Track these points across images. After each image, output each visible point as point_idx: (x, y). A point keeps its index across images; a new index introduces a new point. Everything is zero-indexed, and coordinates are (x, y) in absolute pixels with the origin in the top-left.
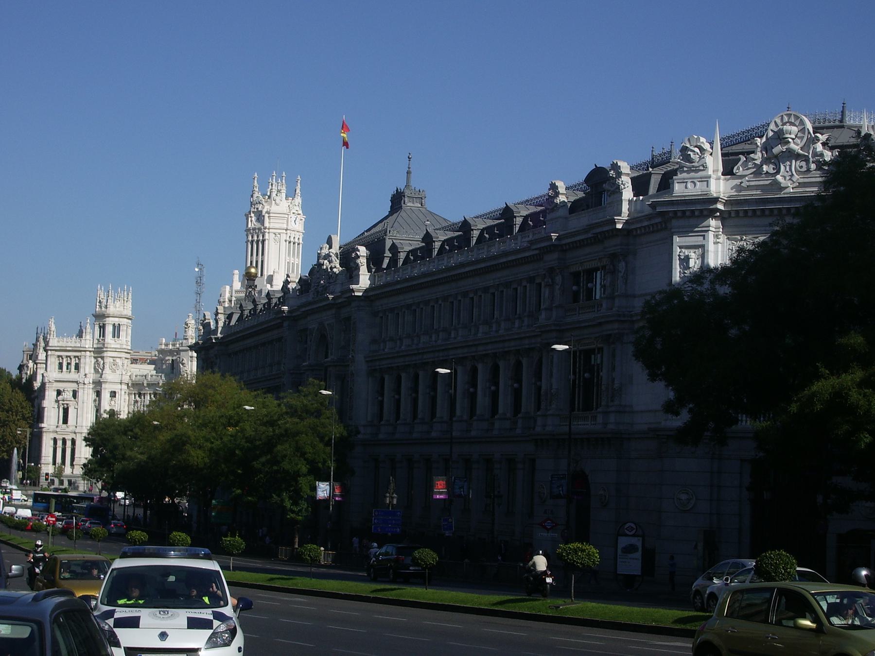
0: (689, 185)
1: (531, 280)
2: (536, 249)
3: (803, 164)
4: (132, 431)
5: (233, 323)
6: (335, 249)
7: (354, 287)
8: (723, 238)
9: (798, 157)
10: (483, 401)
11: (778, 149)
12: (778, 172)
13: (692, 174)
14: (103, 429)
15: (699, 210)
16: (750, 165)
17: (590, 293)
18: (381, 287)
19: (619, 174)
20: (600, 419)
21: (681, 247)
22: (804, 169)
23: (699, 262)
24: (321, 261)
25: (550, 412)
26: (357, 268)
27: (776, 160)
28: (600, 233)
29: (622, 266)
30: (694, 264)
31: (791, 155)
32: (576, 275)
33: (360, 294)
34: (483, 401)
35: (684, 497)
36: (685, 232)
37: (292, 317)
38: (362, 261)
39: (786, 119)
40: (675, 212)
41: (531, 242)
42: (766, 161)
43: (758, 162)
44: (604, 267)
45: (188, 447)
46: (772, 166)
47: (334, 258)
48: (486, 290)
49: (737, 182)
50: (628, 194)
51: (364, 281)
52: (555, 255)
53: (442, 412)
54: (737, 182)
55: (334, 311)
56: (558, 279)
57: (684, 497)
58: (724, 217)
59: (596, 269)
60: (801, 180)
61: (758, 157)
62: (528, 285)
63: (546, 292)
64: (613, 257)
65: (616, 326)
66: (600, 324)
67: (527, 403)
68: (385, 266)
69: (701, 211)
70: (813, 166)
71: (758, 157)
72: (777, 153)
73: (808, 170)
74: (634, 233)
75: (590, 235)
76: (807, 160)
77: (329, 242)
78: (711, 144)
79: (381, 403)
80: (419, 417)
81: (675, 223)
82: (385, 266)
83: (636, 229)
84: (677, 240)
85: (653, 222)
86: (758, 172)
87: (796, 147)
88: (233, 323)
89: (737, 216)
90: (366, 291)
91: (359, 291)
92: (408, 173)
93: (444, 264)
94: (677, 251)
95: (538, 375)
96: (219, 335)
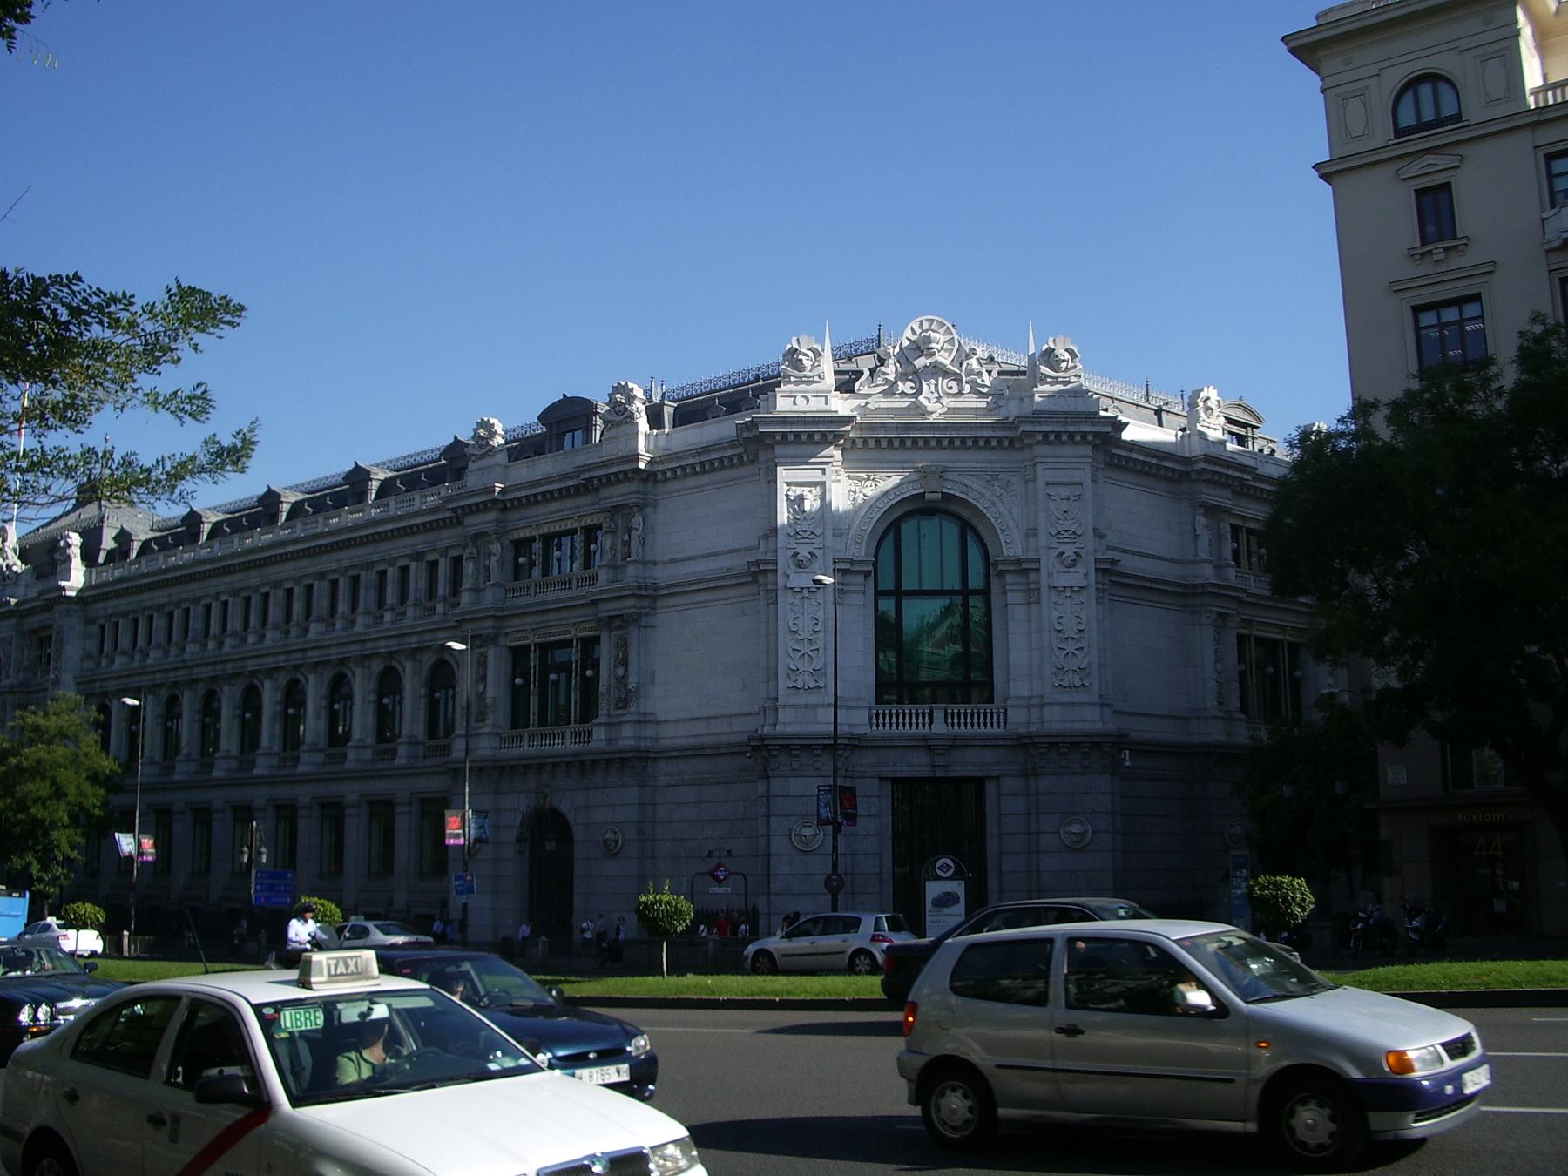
0: (799, 400)
3: (953, 384)
7: (63, 583)
8: (843, 475)
9: (946, 373)
11: (920, 362)
12: (920, 392)
13: (803, 387)
15: (812, 436)
16: (880, 380)
18: (96, 587)
19: (631, 398)
20: (599, 734)
21: (788, 484)
22: (955, 390)
23: (817, 504)
25: (486, 730)
26: (68, 559)
27: (916, 376)
29: (637, 521)
30: (811, 504)
31: (938, 371)
32: (522, 546)
33: (73, 594)
36: (800, 461)
38: (75, 552)
39: (926, 326)
40: (785, 435)
41: (448, 499)
42: (903, 377)
43: (891, 377)
46: (910, 384)
47: (10, 553)
49: (862, 402)
50: (643, 425)
51: (76, 578)
52: (492, 515)
53: (229, 738)
54: (862, 402)
55: (13, 621)
57: (808, 832)
58: (850, 448)
60: (952, 405)
61: (890, 370)
62: (413, 565)
65: (630, 602)
66: (595, 603)
68: (101, 560)
69: (824, 435)
70: (967, 388)
71: (890, 370)
72: (916, 363)
73: (960, 393)
76: (959, 380)
80: (184, 751)
81: (779, 450)
82: (101, 560)
84: (783, 474)
86: (890, 390)
87: (944, 359)
89: (872, 445)
91: (71, 589)
93: (218, 549)
94: (782, 489)
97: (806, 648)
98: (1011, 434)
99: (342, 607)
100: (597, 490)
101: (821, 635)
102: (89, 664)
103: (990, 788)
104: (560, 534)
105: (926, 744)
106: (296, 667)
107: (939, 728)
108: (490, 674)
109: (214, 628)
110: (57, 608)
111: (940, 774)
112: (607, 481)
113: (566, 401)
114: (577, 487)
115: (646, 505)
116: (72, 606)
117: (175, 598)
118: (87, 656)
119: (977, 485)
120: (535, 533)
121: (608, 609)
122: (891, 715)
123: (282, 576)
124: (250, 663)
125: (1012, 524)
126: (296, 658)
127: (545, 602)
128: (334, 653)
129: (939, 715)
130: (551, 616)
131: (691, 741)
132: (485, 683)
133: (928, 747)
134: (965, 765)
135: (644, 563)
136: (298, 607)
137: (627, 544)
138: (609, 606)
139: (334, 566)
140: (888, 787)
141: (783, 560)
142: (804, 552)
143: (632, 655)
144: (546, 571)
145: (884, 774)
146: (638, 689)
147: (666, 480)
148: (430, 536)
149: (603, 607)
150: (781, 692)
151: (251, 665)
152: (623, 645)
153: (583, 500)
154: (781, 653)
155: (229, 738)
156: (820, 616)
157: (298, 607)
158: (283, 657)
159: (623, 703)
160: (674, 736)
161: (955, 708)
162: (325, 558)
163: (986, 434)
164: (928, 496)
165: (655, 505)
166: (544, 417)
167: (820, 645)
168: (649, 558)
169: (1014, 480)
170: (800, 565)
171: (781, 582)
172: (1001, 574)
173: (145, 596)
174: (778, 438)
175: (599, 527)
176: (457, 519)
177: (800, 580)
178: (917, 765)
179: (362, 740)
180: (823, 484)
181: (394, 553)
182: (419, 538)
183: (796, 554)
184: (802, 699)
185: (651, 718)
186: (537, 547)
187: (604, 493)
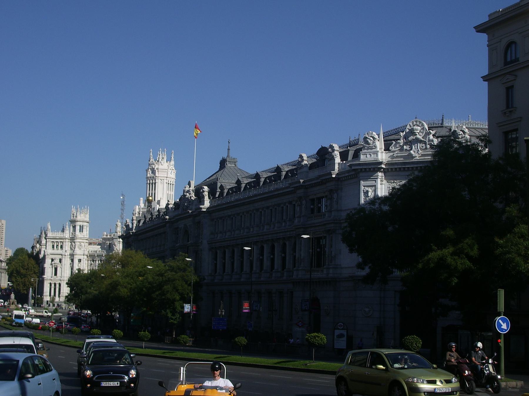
0: (368, 156)
1: (290, 203)
3: (424, 145)
4: (90, 279)
5: (141, 225)
6: (192, 188)
7: (202, 206)
8: (385, 182)
9: (421, 142)
10: (267, 263)
11: (411, 138)
12: (411, 149)
13: (369, 150)
14: (76, 278)
15: (373, 168)
16: (398, 146)
17: (319, 209)
19: (333, 150)
21: (364, 186)
22: (424, 148)
23: (373, 194)
24: (185, 194)
25: (300, 268)
26: (203, 197)
27: (410, 143)
29: (335, 196)
30: (371, 194)
31: (417, 141)
32: (313, 200)
33: (205, 210)
34: (267, 263)
35: (367, 310)
36: (366, 179)
37: (171, 222)
38: (206, 194)
39: (415, 123)
40: (361, 169)
41: (290, 184)
42: (405, 144)
43: (401, 144)
44: (326, 196)
45: (119, 287)
46: (408, 146)
47: (191, 192)
48: (268, 208)
49: (392, 154)
50: (338, 160)
51: (207, 203)
53: (246, 268)
54: (392, 154)
56: (304, 202)
57: (367, 310)
58: (385, 171)
60: (423, 153)
61: (401, 142)
63: (298, 209)
64: (331, 191)
68: (217, 196)
69: (374, 168)
70: (428, 146)
71: (401, 142)
72: (411, 140)
73: (426, 148)
75: (319, 181)
76: (425, 143)
77: (189, 184)
78: (378, 135)
79: (216, 264)
82: (217, 196)
84: (362, 183)
86: (402, 149)
87: (420, 137)
88: (141, 225)
89: (392, 171)
90: (208, 208)
92: (229, 149)
94: (362, 188)
95: (294, 250)
96: (134, 231)
155: (246, 268)
166: (317, 153)
174: (359, 170)
180: (375, 186)
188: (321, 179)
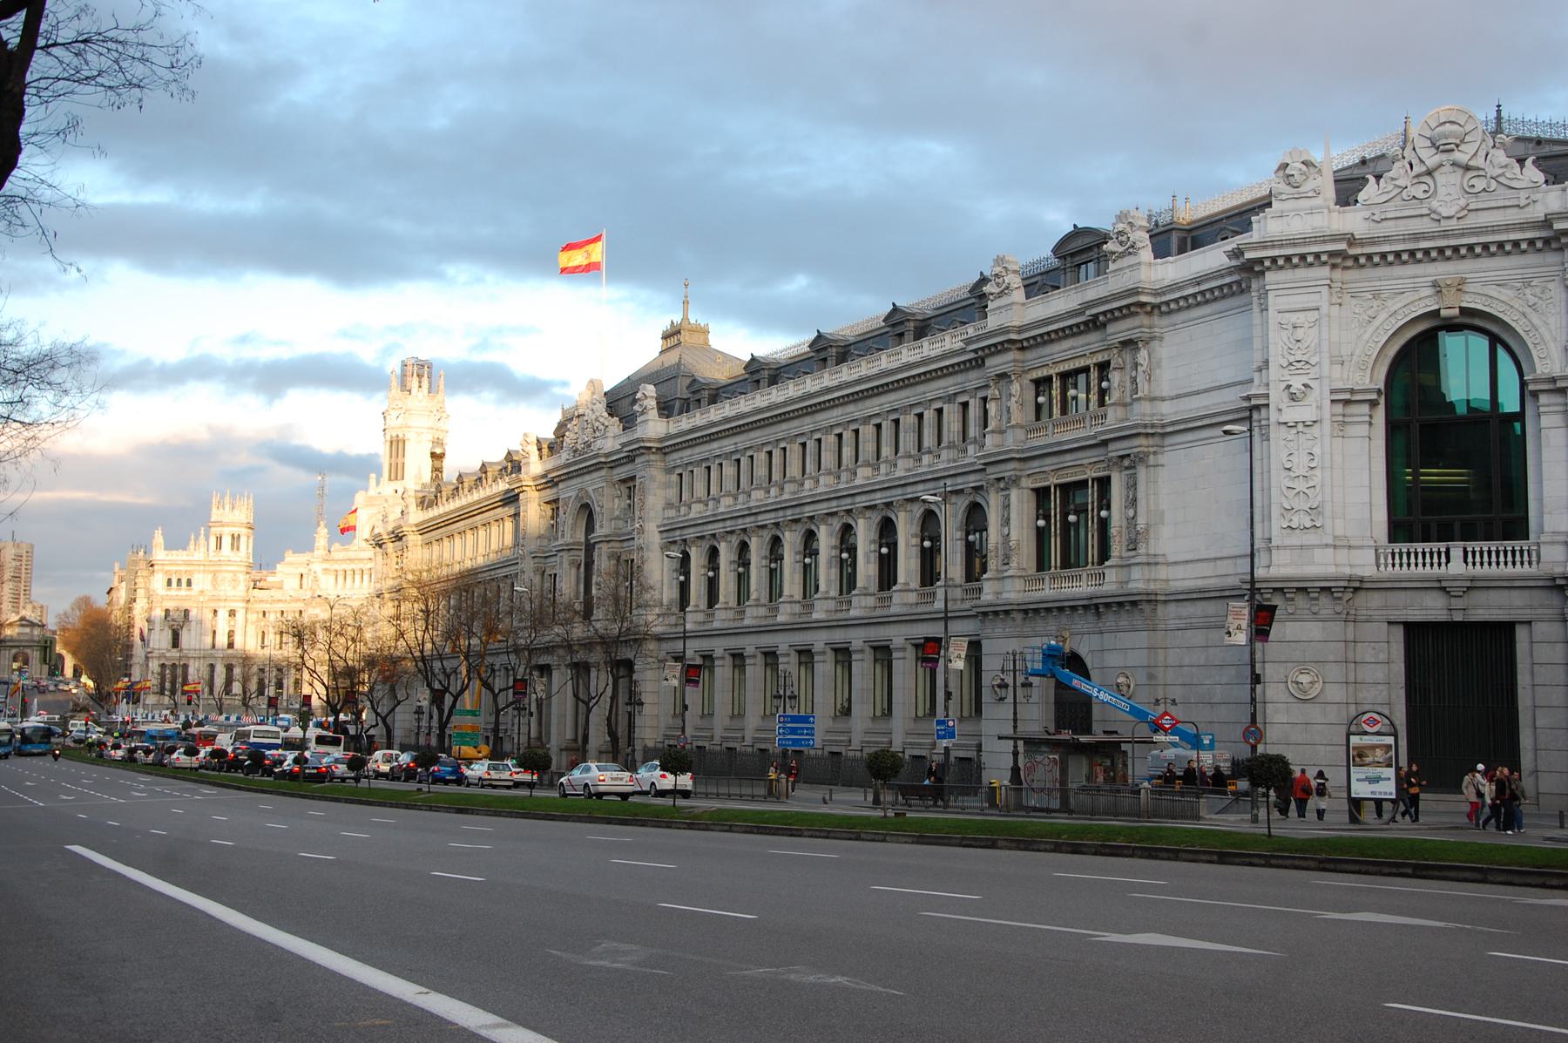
2: (975, 351)
10: (867, 570)
20: (1111, 576)
25: (1010, 573)
28: (1104, 313)
32: (1042, 384)
35: (1305, 679)
40: (1274, 260)
41: (968, 341)
44: (1104, 367)
55: (603, 472)
57: (1305, 679)
59: (1086, 370)
66: (1105, 443)
67: (953, 564)
74: (1164, 308)
80: (753, 596)
83: (1167, 303)
85: (1204, 287)
97: (1301, 485)
98: (1544, 234)
99: (886, 451)
100: (1104, 325)
101: (1318, 472)
102: (672, 513)
103: (1521, 634)
104: (1077, 371)
105: (1442, 587)
106: (849, 512)
107: (1457, 567)
108: (1013, 516)
109: (776, 476)
110: (638, 460)
111: (1458, 617)
112: (1114, 316)
113: (1077, 233)
114: (1085, 323)
115: (1152, 338)
116: (652, 457)
117: (740, 446)
118: (669, 505)
119: (1506, 294)
120: (1052, 372)
121: (1116, 449)
122: (1409, 554)
123: (833, 422)
124: (807, 508)
125: (1547, 336)
126: (846, 504)
127: (1060, 443)
128: (878, 498)
129: (1456, 553)
130: (1068, 457)
131: (1200, 583)
132: (1013, 523)
133: (1443, 589)
134: (1486, 608)
135: (1153, 399)
136: (848, 452)
137: (1134, 380)
138: (1118, 445)
139: (876, 410)
140: (1399, 633)
141: (1277, 396)
142: (1297, 384)
143: (1141, 495)
144: (1064, 411)
145: (1393, 618)
146: (1147, 530)
147: (1170, 312)
148: (959, 378)
149: (1112, 447)
150: (1274, 533)
151: (808, 511)
152: (1132, 485)
153: (1093, 337)
154: (1274, 492)
156: (1317, 451)
157: (848, 452)
158: (834, 503)
159: (1133, 545)
160: (1183, 578)
161: (1476, 545)
162: (868, 403)
163: (1513, 236)
164: (1444, 313)
165: (1161, 339)
167: (1316, 481)
168: (1157, 394)
169: (1550, 285)
170: (1293, 398)
171: (1273, 419)
172: (1535, 394)
173: (715, 445)
175: (1108, 363)
176: (978, 362)
177: (1291, 415)
178: (1431, 608)
179: (907, 584)
181: (929, 396)
182: (951, 380)
183: (1289, 387)
184: (1296, 539)
185: (1160, 560)
186: (1056, 384)
187: (1111, 328)
188: (1094, 311)
